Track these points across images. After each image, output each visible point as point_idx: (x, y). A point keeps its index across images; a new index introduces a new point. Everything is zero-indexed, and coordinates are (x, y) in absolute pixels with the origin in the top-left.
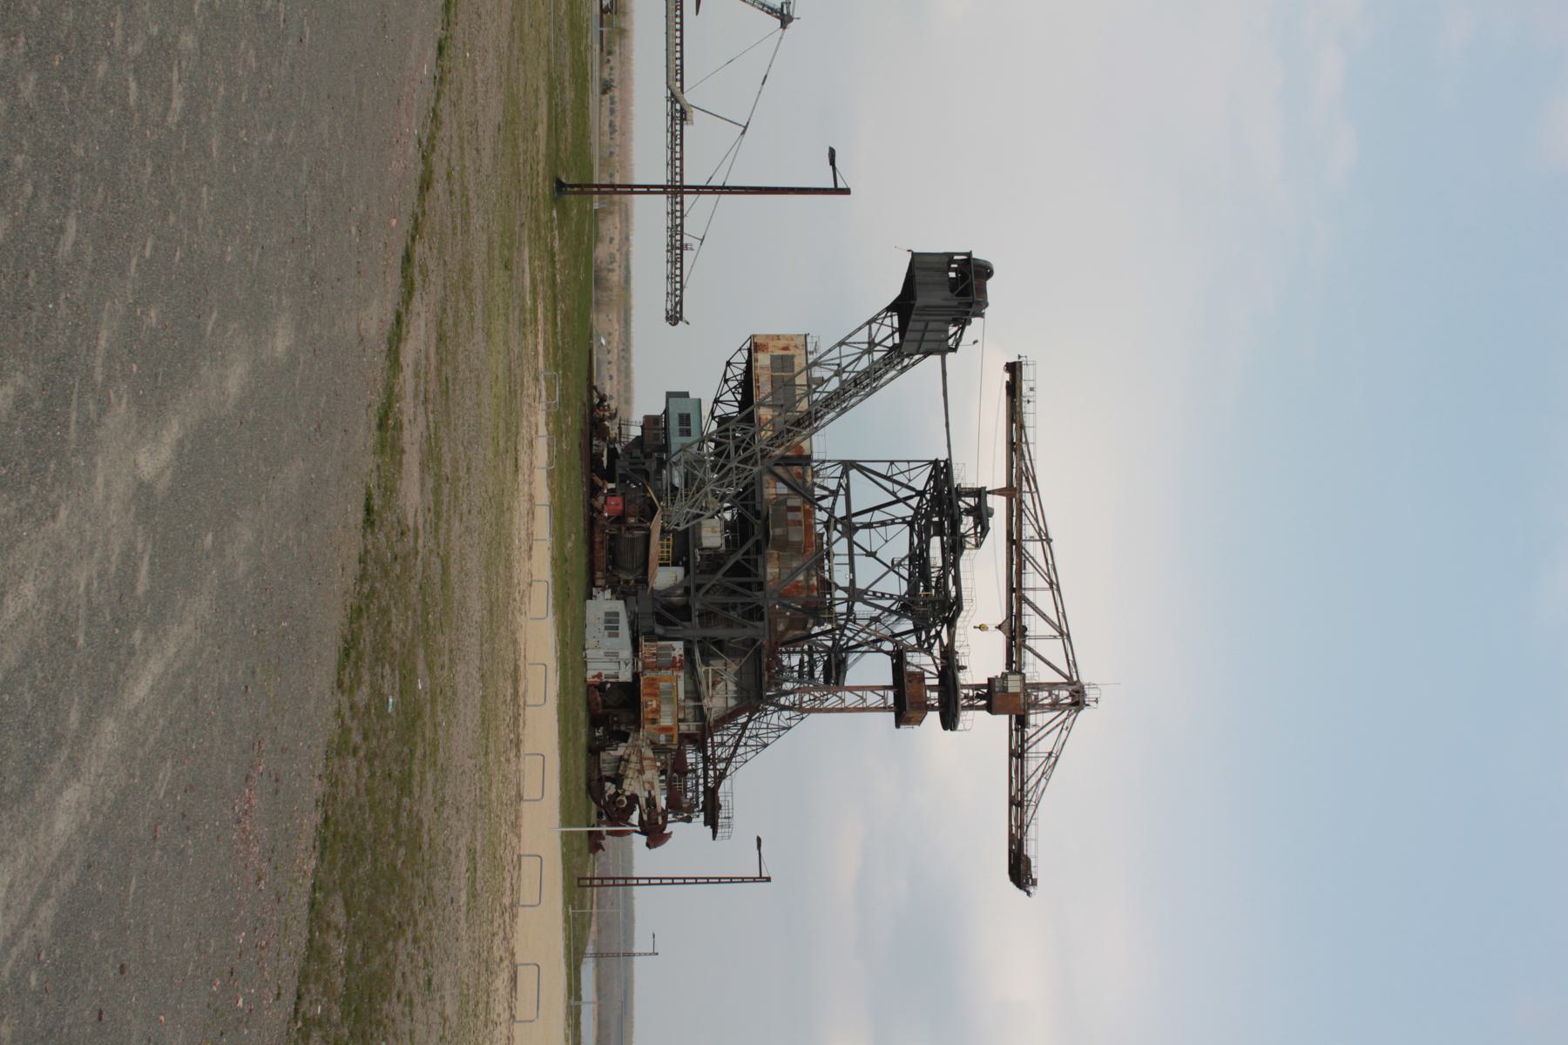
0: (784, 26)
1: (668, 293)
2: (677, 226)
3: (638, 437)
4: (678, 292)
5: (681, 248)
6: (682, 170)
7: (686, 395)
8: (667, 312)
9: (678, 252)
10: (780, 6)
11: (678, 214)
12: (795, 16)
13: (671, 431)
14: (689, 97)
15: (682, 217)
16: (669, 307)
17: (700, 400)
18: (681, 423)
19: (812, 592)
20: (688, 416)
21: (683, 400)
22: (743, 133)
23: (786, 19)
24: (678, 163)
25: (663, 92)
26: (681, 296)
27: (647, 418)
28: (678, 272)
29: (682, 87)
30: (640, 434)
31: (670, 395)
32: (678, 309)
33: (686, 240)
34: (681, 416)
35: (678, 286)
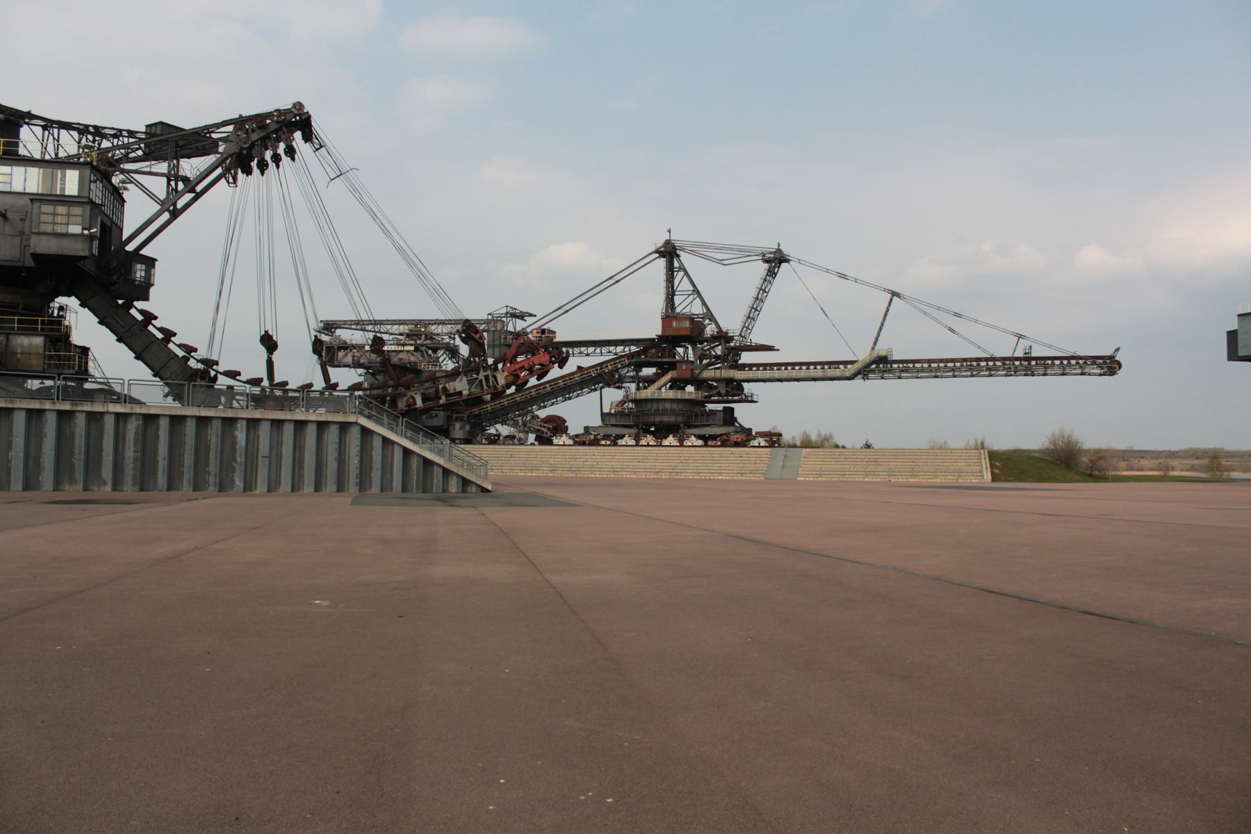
0: (787, 261)
1: (1082, 374)
2: (1004, 364)
4: (1081, 362)
5: (1028, 359)
6: (941, 361)
8: (1104, 374)
9: (1033, 363)
10: (766, 266)
11: (991, 363)
12: (777, 247)
14: (863, 354)
15: (994, 359)
22: (898, 295)
23: (778, 256)
24: (934, 365)
25: (858, 382)
26: (1086, 358)
28: (1057, 362)
29: (852, 362)
32: (1101, 361)
33: (1020, 354)
35: (1073, 362)
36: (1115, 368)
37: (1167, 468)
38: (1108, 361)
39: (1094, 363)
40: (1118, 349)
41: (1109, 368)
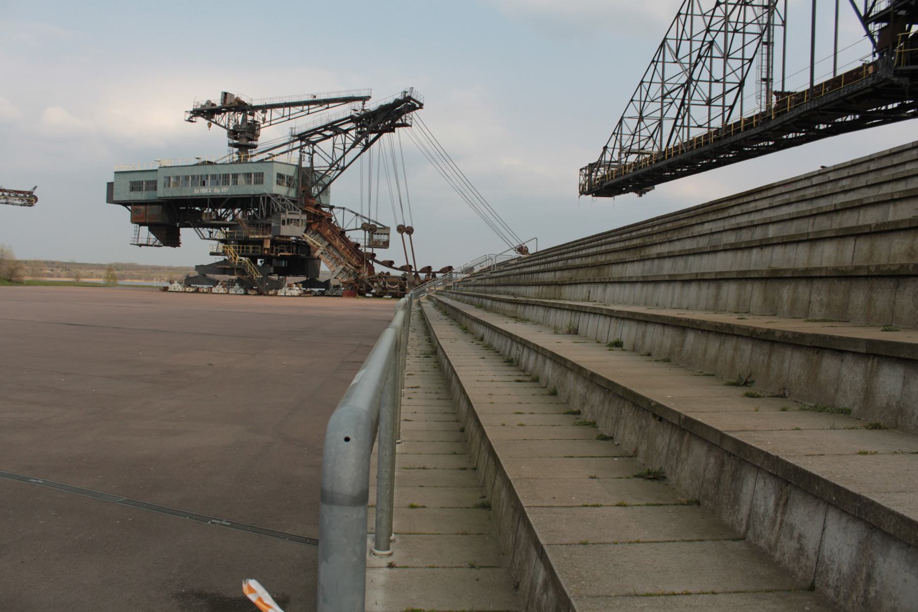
1: (7, 203)
3: (150, 230)
4: (6, 194)
7: (110, 186)
13: (152, 198)
16: (20, 202)
17: (116, 173)
18: (140, 189)
19: (250, 113)
20: (132, 183)
21: (115, 187)
26: (10, 191)
27: (134, 220)
30: (147, 228)
31: (110, 200)
34: (132, 189)
36: (33, 201)
37: (78, 277)
38: (28, 196)
39: (16, 196)
40: (35, 188)
41: (28, 200)
